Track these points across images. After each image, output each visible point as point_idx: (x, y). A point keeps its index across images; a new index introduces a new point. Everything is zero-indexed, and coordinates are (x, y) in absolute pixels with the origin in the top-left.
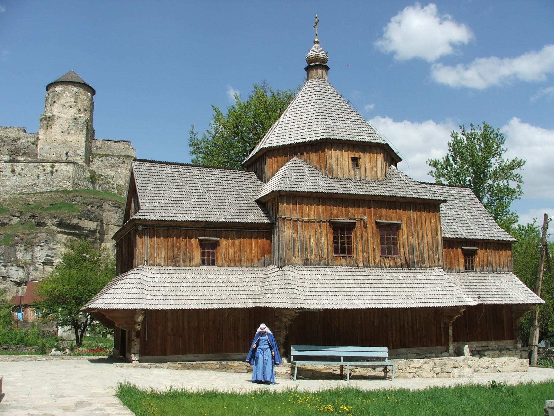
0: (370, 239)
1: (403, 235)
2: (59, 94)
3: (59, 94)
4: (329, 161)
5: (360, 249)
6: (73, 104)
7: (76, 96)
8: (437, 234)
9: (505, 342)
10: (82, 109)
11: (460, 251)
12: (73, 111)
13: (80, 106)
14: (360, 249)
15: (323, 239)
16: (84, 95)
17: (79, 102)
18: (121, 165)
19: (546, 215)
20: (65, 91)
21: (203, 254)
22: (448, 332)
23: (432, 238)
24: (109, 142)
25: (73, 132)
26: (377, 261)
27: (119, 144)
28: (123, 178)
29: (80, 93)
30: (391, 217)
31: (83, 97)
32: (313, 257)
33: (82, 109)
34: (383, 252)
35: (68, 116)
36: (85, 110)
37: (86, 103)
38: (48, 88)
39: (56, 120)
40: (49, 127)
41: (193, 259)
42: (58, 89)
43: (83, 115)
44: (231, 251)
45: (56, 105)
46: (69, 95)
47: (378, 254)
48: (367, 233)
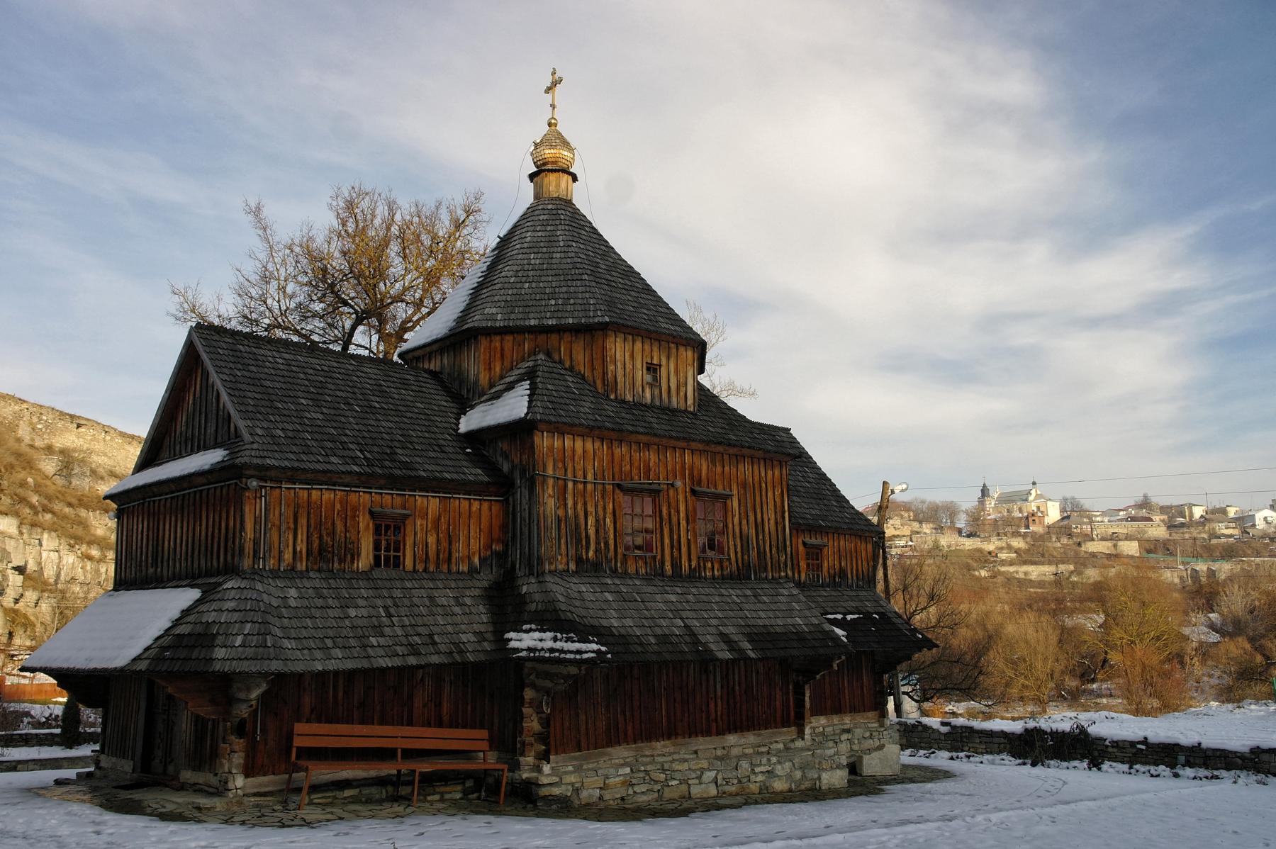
0: (683, 523)
4: (611, 367)
5: (667, 541)
8: (783, 518)
11: (801, 548)
14: (667, 541)
15: (608, 520)
19: (885, 483)
21: (377, 547)
22: (804, 701)
23: (776, 523)
26: (694, 564)
32: (591, 554)
41: (359, 555)
44: (431, 540)
48: (678, 512)
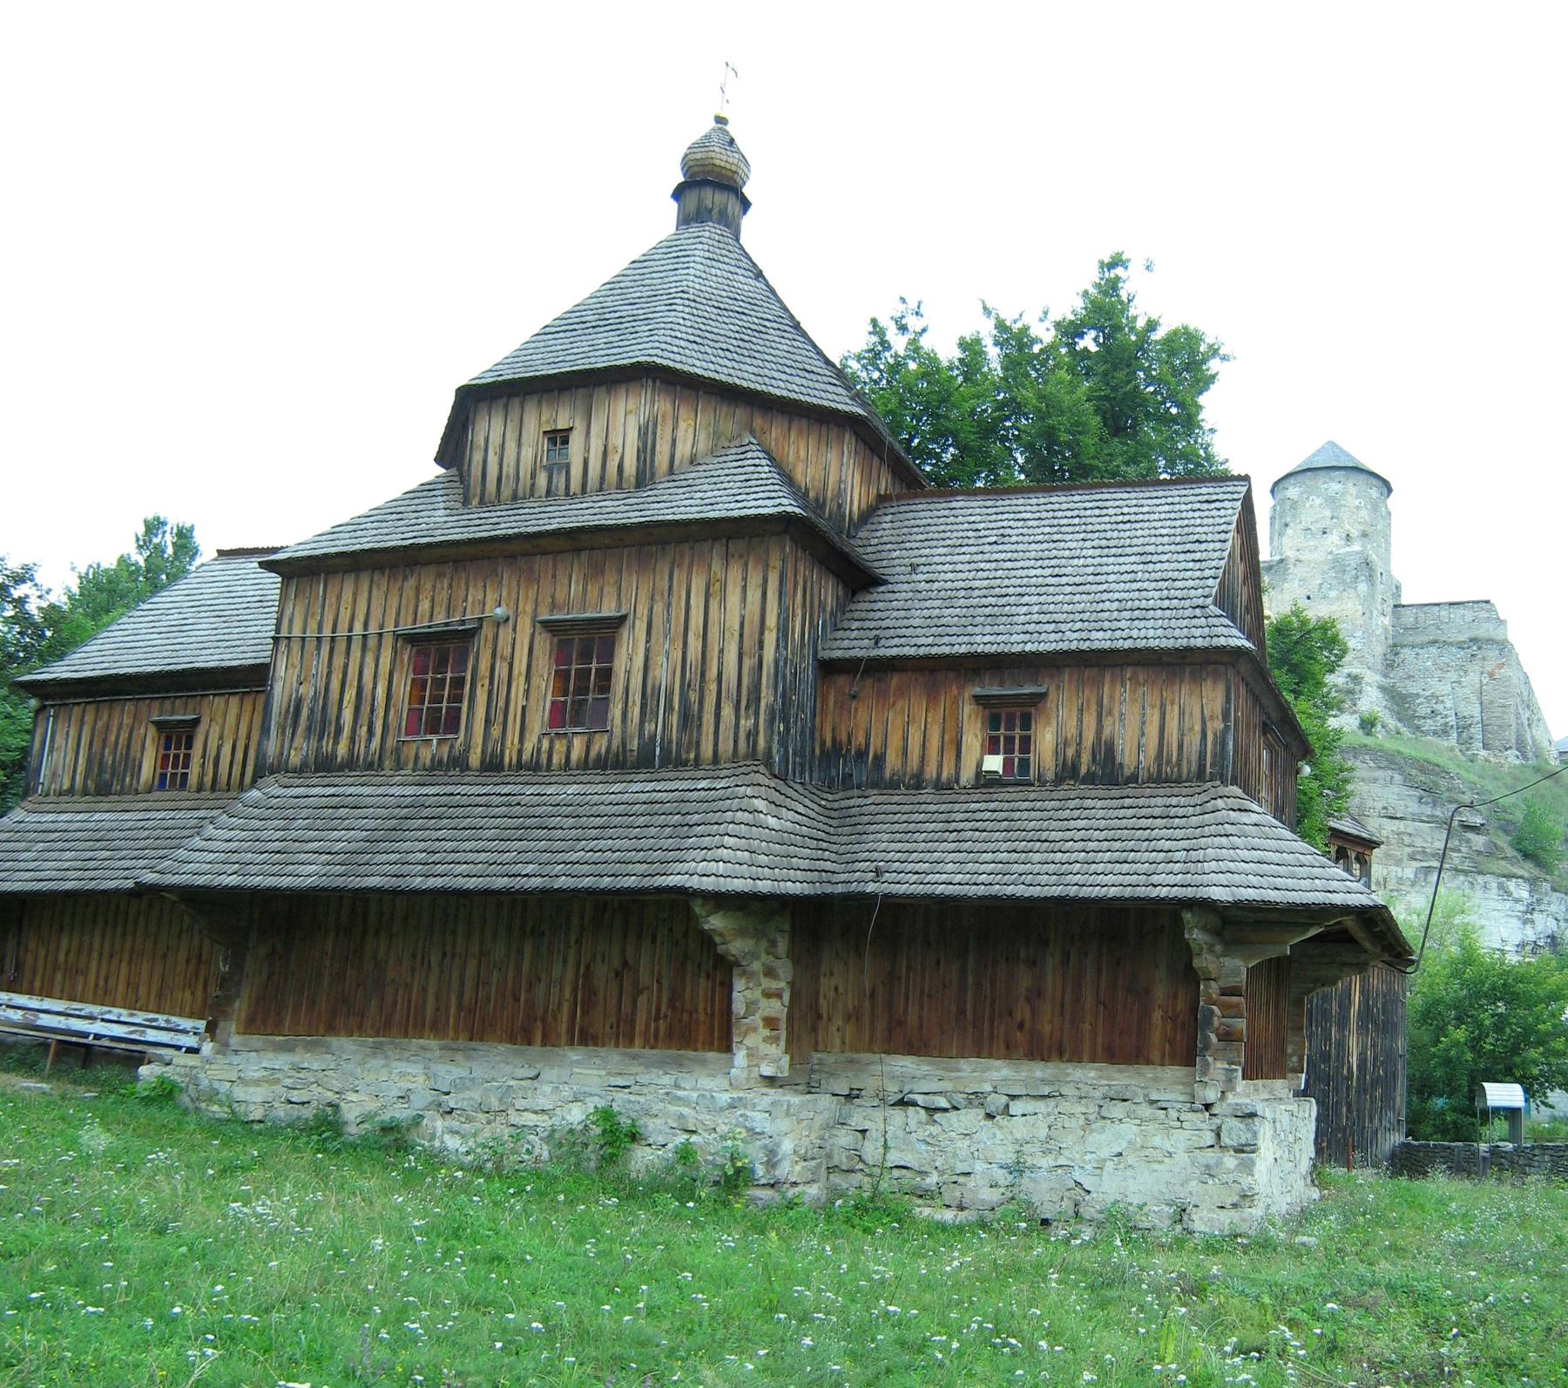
1: (628, 656)
2: (1294, 505)
3: (1294, 505)
6: (1328, 522)
7: (1333, 501)
9: (1149, 1072)
10: (1355, 533)
12: (1334, 539)
13: (1347, 526)
17: (1344, 515)
18: (1469, 666)
20: (1310, 494)
24: (1436, 609)
25: (1333, 594)
26: (529, 746)
27: (1461, 611)
28: (1474, 698)
29: (1345, 493)
34: (558, 716)
35: (1319, 556)
36: (1365, 535)
37: (1364, 513)
38: (1272, 491)
42: (1293, 492)
43: (1356, 547)
45: (1289, 531)
46: (1318, 501)
47: (537, 723)
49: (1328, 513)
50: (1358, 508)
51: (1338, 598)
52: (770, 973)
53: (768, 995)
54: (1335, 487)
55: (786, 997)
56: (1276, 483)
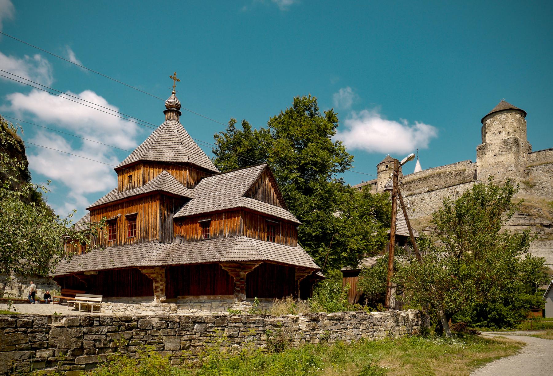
7: (503, 122)
10: (511, 131)
16: (512, 118)
17: (507, 126)
29: (507, 118)
30: (132, 210)
31: (512, 121)
33: (511, 131)
36: (515, 131)
37: (515, 124)
38: (482, 122)
39: (489, 147)
40: (484, 153)
42: (488, 121)
45: (487, 135)
49: (501, 126)
50: (512, 122)
51: (505, 154)
52: (161, 281)
53: (161, 285)
54: (503, 116)
55: (165, 285)
56: (483, 119)
